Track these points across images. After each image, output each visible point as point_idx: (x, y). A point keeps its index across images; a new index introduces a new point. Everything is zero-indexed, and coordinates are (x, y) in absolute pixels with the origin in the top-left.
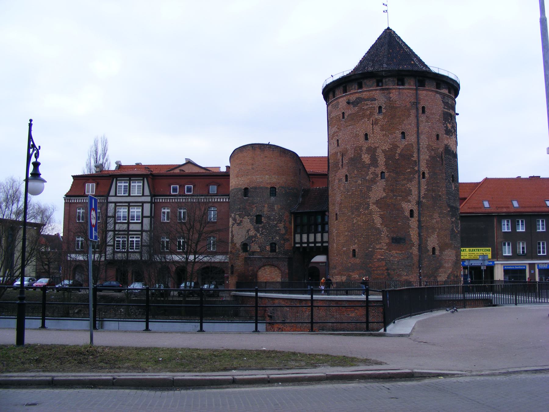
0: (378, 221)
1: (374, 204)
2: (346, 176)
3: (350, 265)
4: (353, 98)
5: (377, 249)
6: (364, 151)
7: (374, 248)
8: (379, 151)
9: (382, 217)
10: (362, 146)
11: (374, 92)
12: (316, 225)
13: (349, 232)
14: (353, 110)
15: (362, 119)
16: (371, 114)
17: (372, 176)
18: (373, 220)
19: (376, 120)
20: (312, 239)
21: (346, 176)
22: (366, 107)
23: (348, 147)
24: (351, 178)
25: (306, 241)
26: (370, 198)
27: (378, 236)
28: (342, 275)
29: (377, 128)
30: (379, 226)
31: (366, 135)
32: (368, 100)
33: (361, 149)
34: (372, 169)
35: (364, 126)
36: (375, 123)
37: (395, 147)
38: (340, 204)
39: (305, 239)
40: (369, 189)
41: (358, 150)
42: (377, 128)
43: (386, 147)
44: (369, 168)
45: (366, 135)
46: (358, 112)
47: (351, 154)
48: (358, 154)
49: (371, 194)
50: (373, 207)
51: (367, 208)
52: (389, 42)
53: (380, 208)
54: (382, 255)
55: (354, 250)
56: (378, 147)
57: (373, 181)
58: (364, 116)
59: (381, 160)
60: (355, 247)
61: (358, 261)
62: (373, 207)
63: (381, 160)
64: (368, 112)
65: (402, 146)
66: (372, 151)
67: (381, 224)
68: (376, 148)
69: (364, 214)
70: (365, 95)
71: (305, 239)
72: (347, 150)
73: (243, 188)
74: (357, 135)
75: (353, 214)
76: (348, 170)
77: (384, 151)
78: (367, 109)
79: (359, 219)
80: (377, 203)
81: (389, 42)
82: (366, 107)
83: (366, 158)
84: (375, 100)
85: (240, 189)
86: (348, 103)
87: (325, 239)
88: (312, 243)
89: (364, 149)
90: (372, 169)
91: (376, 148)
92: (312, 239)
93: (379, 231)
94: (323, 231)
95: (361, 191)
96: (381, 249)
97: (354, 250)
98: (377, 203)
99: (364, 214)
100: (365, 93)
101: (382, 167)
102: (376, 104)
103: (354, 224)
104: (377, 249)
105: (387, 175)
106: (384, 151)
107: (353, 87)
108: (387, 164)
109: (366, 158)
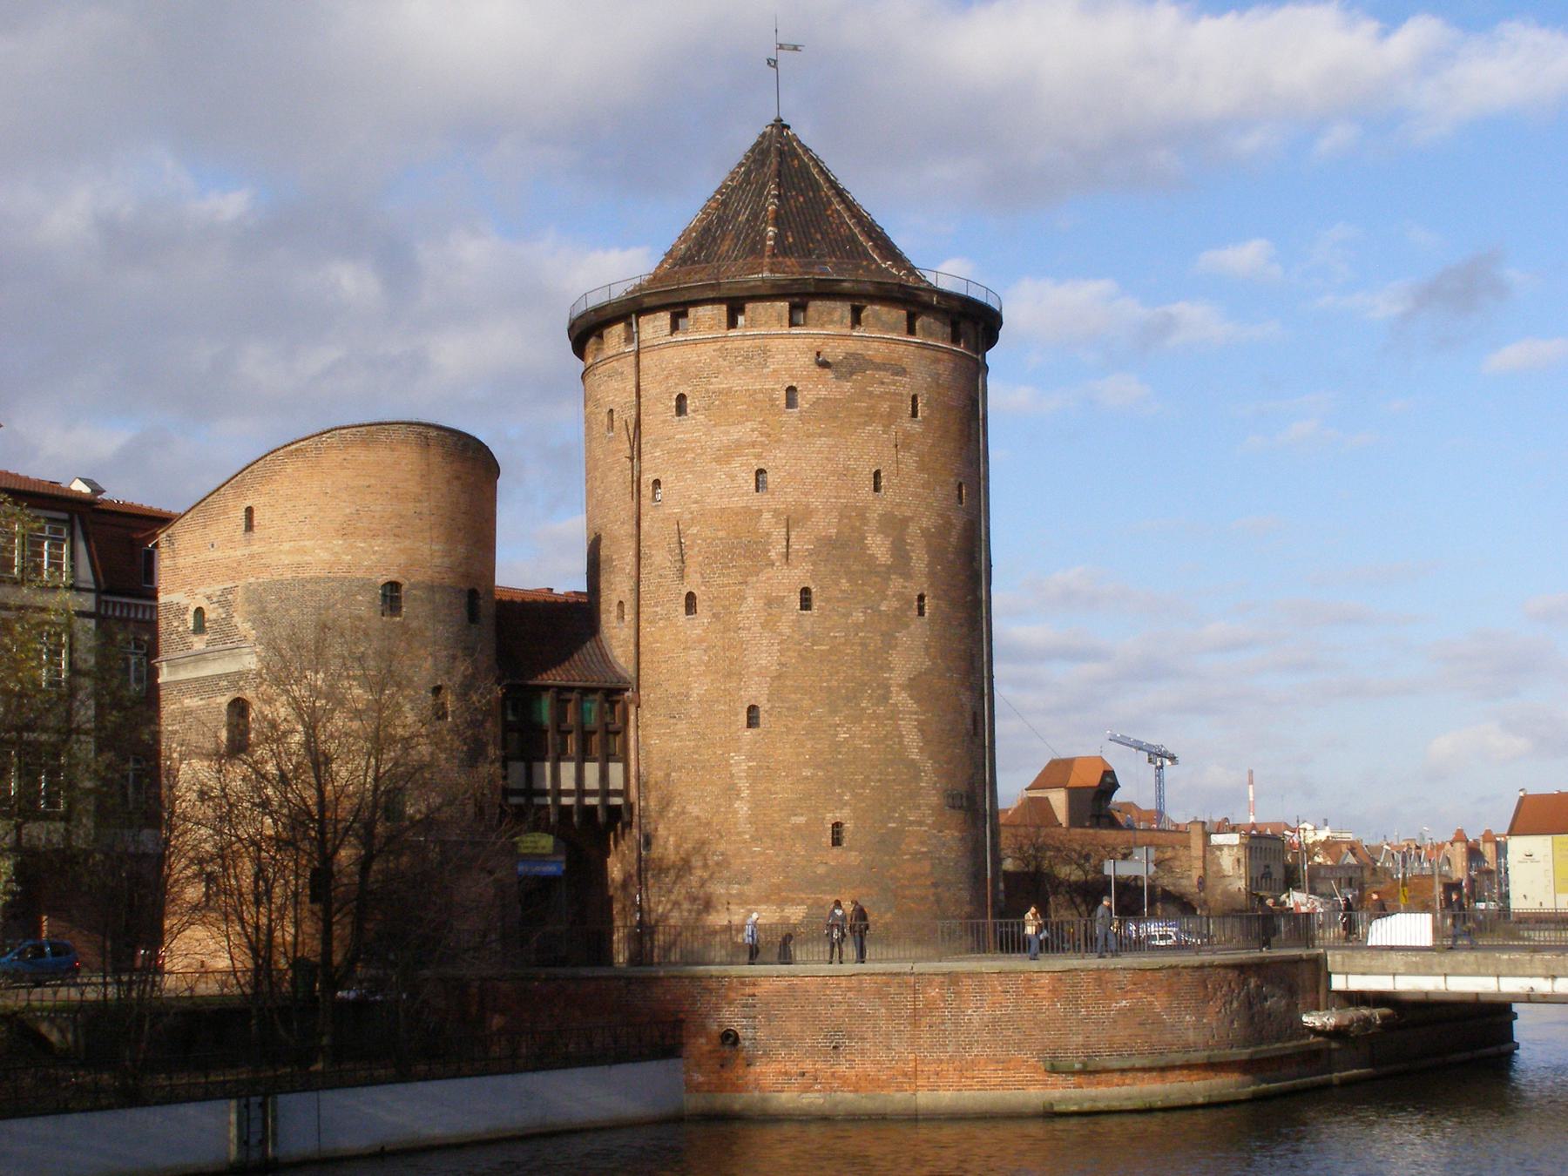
1: (902, 687)
2: (805, 592)
3: (821, 870)
5: (911, 823)
6: (874, 524)
7: (902, 819)
8: (913, 529)
9: (922, 728)
10: (866, 508)
11: (901, 348)
12: (585, 736)
13: (818, 766)
15: (866, 424)
17: (896, 604)
18: (901, 736)
19: (907, 435)
21: (805, 592)
22: (877, 389)
23: (815, 502)
24: (828, 600)
26: (892, 670)
27: (913, 786)
28: (782, 903)
30: (914, 755)
31: (877, 474)
33: (862, 515)
38: (779, 677)
39: (567, 782)
40: (889, 641)
41: (853, 517)
42: (910, 461)
44: (887, 579)
45: (877, 474)
47: (825, 525)
48: (853, 528)
49: (895, 658)
50: (901, 698)
51: (885, 698)
53: (918, 701)
54: (923, 843)
55: (837, 826)
56: (911, 518)
58: (870, 416)
60: (838, 816)
61: (850, 857)
63: (920, 560)
64: (885, 407)
67: (921, 750)
70: (876, 351)
71: (567, 782)
72: (808, 513)
73: (382, 580)
75: (834, 711)
76: (814, 575)
77: (925, 532)
78: (881, 396)
79: (857, 729)
80: (912, 685)
82: (877, 389)
84: (903, 372)
85: (365, 585)
87: (616, 781)
88: (593, 793)
89: (873, 516)
90: (896, 583)
91: (905, 521)
94: (606, 758)
95: (863, 645)
96: (920, 823)
97: (837, 826)
99: (875, 716)
100: (876, 345)
102: (905, 386)
103: (840, 744)
104: (911, 823)
107: (836, 316)
109: (878, 547)
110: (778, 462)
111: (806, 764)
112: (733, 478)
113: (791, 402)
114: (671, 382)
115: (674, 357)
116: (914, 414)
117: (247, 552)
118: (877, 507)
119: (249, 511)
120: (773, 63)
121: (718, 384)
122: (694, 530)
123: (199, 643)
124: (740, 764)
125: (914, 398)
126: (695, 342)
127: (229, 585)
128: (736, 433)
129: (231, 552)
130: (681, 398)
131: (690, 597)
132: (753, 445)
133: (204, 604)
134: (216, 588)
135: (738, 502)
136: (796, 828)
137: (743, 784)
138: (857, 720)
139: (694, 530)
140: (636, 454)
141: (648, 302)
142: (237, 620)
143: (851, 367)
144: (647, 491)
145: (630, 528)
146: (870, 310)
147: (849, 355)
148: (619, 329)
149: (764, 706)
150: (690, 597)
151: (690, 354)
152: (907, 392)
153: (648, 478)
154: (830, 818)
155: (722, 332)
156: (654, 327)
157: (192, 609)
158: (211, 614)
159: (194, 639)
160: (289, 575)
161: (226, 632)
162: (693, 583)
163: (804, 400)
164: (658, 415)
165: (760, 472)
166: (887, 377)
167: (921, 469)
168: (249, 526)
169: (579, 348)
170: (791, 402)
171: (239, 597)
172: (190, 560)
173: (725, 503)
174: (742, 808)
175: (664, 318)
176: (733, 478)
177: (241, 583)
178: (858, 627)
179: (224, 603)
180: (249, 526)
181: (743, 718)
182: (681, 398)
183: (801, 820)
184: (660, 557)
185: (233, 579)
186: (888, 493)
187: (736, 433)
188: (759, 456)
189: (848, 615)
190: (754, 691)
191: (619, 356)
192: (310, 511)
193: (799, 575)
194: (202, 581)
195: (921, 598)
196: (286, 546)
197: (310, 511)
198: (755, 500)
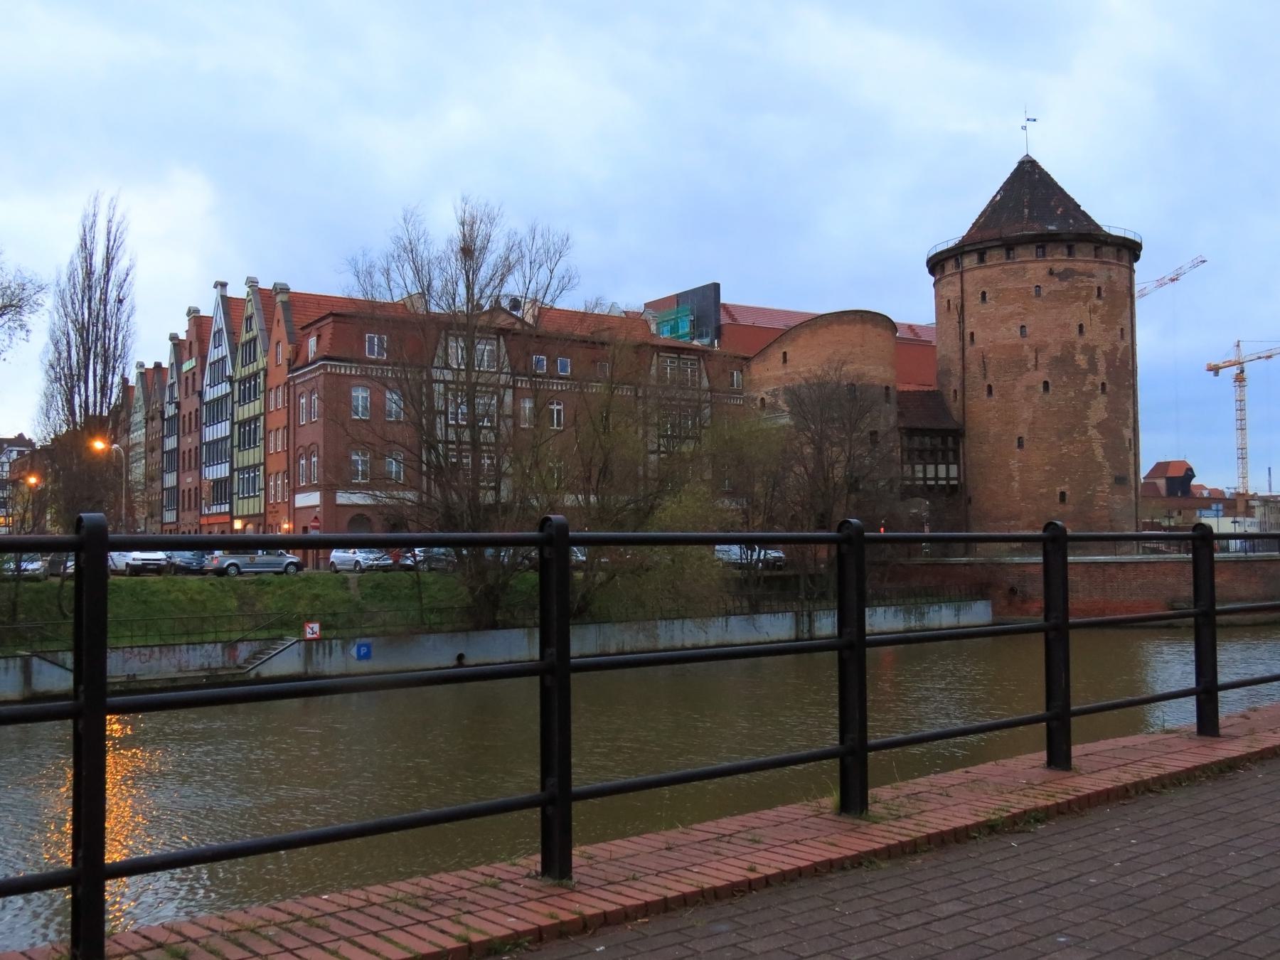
0: (1099, 453)
4: (1059, 267)
8: (1099, 351)
9: (1104, 447)
14: (1056, 285)
16: (1087, 298)
19: (1095, 306)
20: (931, 474)
21: (1046, 383)
23: (1049, 340)
25: (921, 475)
29: (1096, 318)
30: (1100, 459)
31: (1081, 326)
32: (1081, 274)
33: (1074, 348)
34: (1091, 377)
35: (1075, 313)
36: (1093, 310)
37: (1115, 349)
40: (1087, 406)
41: (1069, 348)
42: (1096, 318)
43: (1107, 347)
45: (1081, 326)
46: (1068, 290)
47: (1056, 351)
49: (1090, 413)
50: (1092, 432)
51: (1086, 432)
52: (1029, 183)
53: (1101, 433)
55: (1063, 494)
57: (1091, 395)
58: (1077, 298)
59: (1102, 366)
60: (1063, 488)
62: (1092, 432)
63: (1102, 366)
64: (1084, 293)
65: (1121, 349)
66: (1089, 350)
68: (1095, 348)
69: (1080, 441)
70: (1079, 266)
72: (1047, 346)
74: (1065, 326)
75: (1060, 439)
76: (1050, 375)
77: (1105, 353)
80: (1098, 426)
81: (1029, 183)
82: (1080, 285)
83: (1081, 360)
84: (1093, 276)
86: (1051, 273)
89: (1079, 346)
90: (1091, 377)
91: (1095, 348)
92: (931, 474)
93: (1100, 465)
97: (1063, 494)
98: (1098, 426)
101: (1101, 378)
102: (1095, 283)
105: (1108, 387)
106: (1105, 353)
108: (1107, 373)
109: (1081, 360)
110: (1030, 321)
111: (1047, 464)
113: (1038, 294)
115: (979, 274)
116: (1099, 295)
118: (1080, 342)
120: (1024, 128)
124: (1014, 464)
125: (1099, 289)
128: (1010, 309)
130: (984, 294)
131: (990, 387)
132: (1019, 314)
133: (765, 396)
136: (1042, 495)
137: (1016, 474)
138: (1071, 443)
140: (962, 321)
141: (967, 249)
143: (1065, 275)
144: (968, 338)
145: (959, 355)
146: (1078, 246)
147: (1066, 270)
148: (951, 263)
149: (1026, 437)
150: (990, 387)
151: (988, 272)
152: (1095, 285)
153: (968, 331)
154: (1058, 490)
155: (1004, 261)
156: (970, 261)
161: (774, 408)
162: (991, 380)
163: (1044, 293)
164: (973, 302)
165: (1023, 327)
166: (1084, 278)
167: (1102, 322)
168: (785, 361)
169: (932, 271)
170: (1038, 294)
173: (1006, 342)
174: (1016, 485)
175: (975, 257)
176: (1009, 330)
178: (1072, 399)
179: (774, 394)
180: (785, 361)
181: (1016, 443)
182: (984, 294)
183: (1044, 490)
184: (974, 368)
186: (1087, 335)
187: (1010, 309)
189: (1066, 394)
190: (1022, 431)
191: (952, 275)
193: (1042, 375)
195: (1103, 384)
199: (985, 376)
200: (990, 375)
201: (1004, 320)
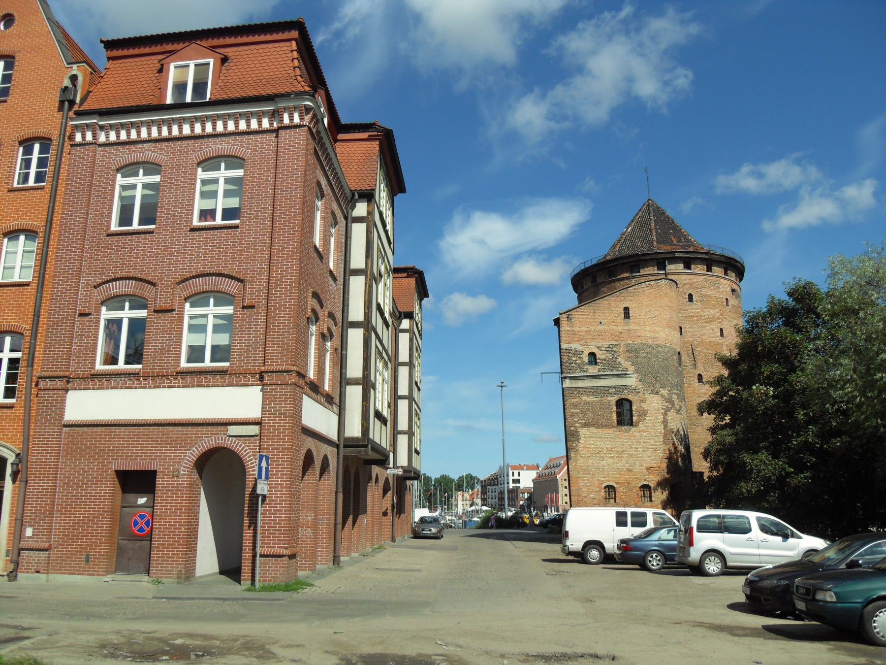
112: (713, 330)
114: (685, 288)
117: (626, 328)
119: (626, 310)
121: (704, 292)
122: (699, 349)
123: (593, 370)
126: (696, 274)
127: (614, 343)
129: (615, 328)
133: (596, 351)
134: (606, 344)
135: (713, 340)
139: (699, 349)
142: (620, 359)
151: (694, 278)
157: (586, 352)
158: (600, 355)
159: (589, 367)
160: (650, 342)
161: (612, 364)
162: (700, 370)
163: (730, 303)
171: (622, 349)
172: (584, 329)
173: (709, 339)
176: (713, 330)
177: (623, 343)
179: (610, 349)
185: (617, 340)
188: (720, 323)
192: (657, 313)
194: (593, 339)
196: (648, 328)
197: (657, 313)
198: (719, 339)
199: (695, 366)
200: (699, 365)
201: (710, 320)
